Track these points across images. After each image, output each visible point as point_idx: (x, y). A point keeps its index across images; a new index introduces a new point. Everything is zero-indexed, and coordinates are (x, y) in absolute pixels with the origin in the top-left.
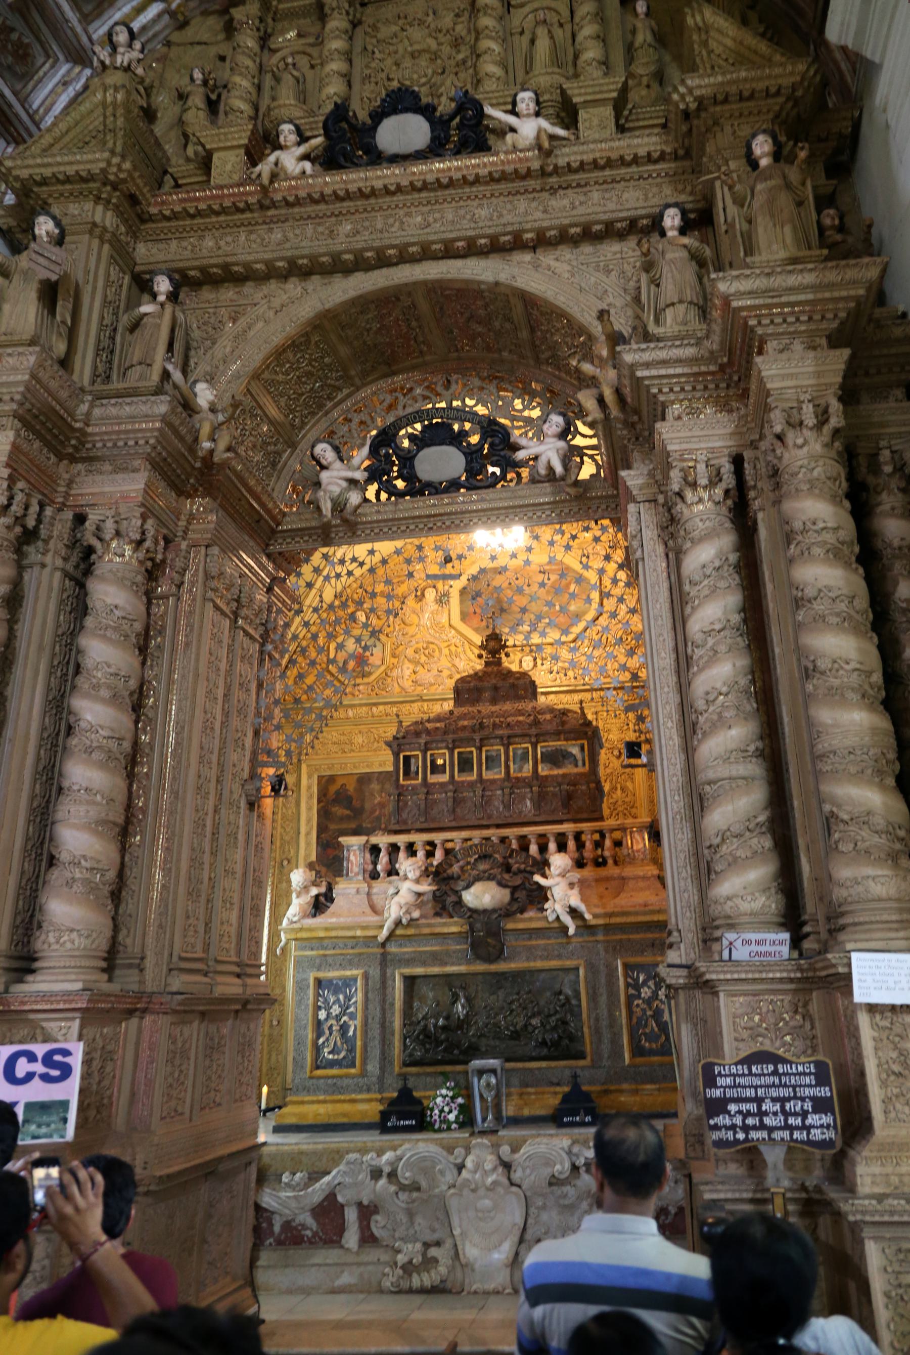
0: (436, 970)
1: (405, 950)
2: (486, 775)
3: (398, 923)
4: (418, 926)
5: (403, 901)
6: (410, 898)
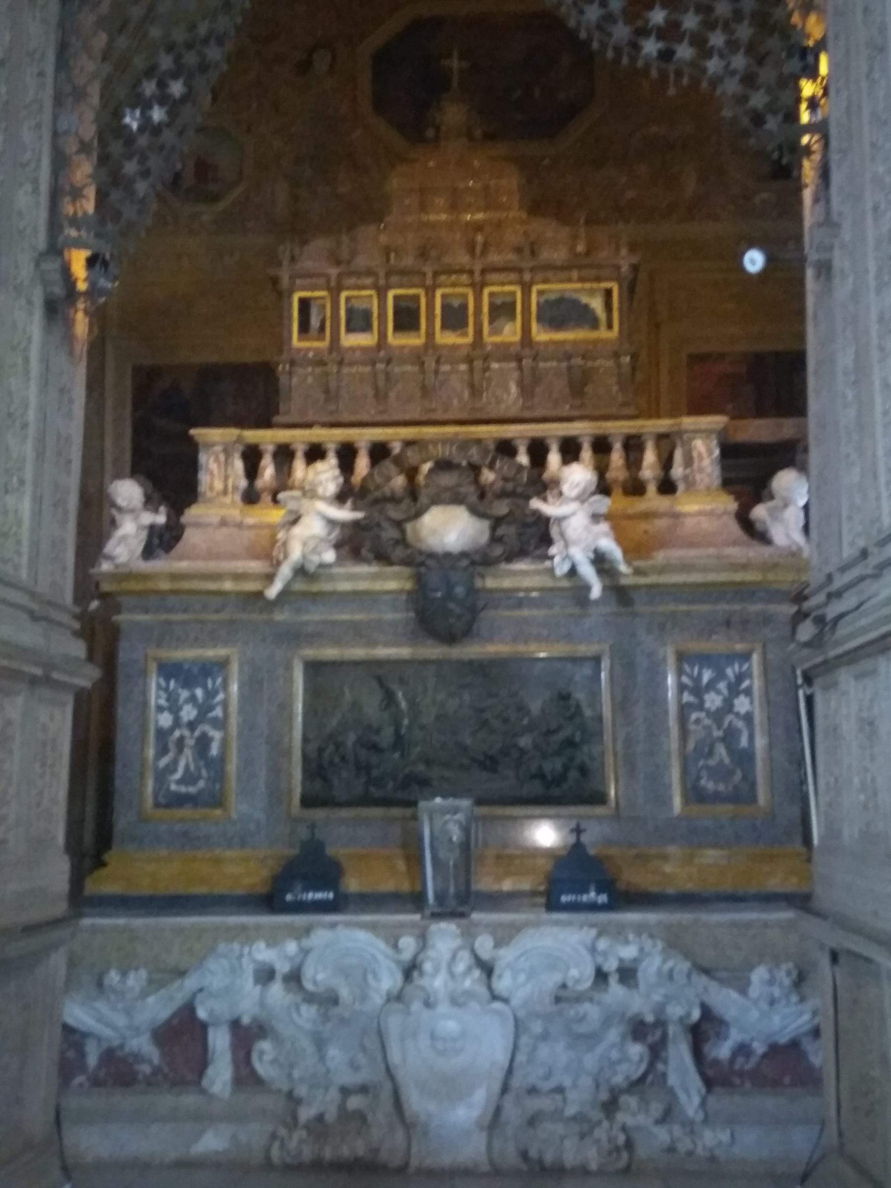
0: (358, 653)
1: (306, 618)
3: (301, 571)
4: (331, 578)
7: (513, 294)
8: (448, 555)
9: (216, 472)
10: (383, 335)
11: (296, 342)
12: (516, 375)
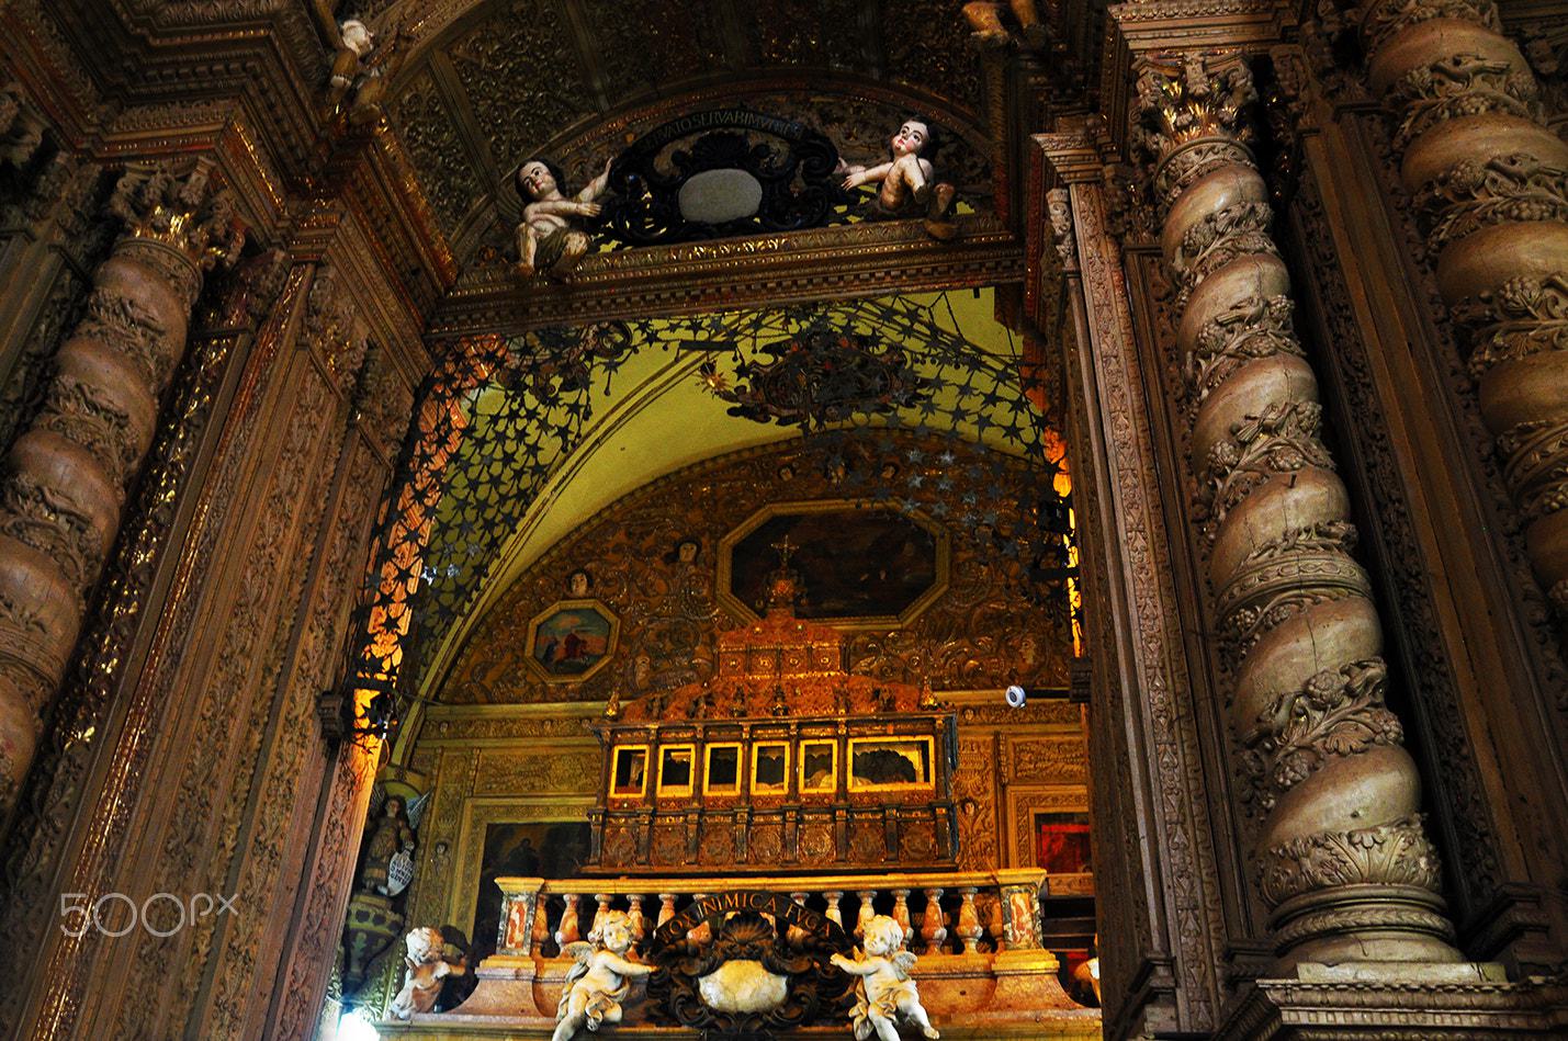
2: (760, 790)
5: (592, 988)
6: (610, 984)
7: (830, 746)
8: (740, 1015)
9: (517, 922)
10: (698, 787)
11: (612, 794)
12: (829, 827)
